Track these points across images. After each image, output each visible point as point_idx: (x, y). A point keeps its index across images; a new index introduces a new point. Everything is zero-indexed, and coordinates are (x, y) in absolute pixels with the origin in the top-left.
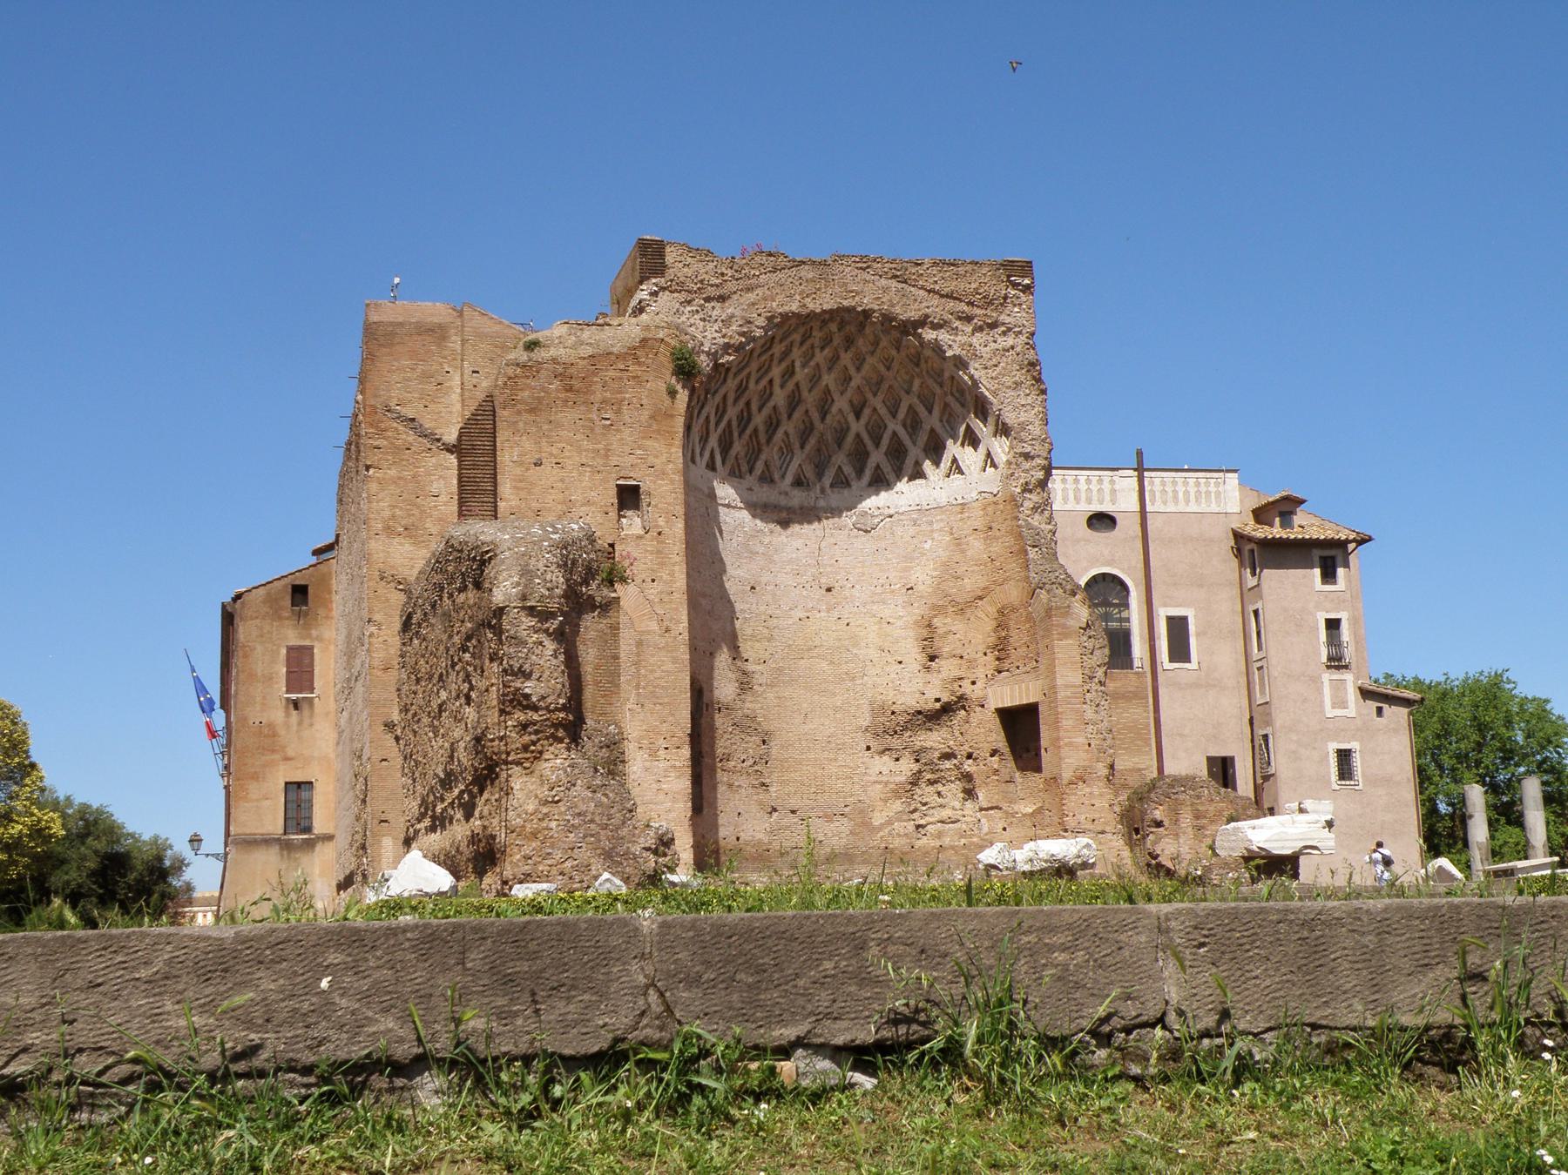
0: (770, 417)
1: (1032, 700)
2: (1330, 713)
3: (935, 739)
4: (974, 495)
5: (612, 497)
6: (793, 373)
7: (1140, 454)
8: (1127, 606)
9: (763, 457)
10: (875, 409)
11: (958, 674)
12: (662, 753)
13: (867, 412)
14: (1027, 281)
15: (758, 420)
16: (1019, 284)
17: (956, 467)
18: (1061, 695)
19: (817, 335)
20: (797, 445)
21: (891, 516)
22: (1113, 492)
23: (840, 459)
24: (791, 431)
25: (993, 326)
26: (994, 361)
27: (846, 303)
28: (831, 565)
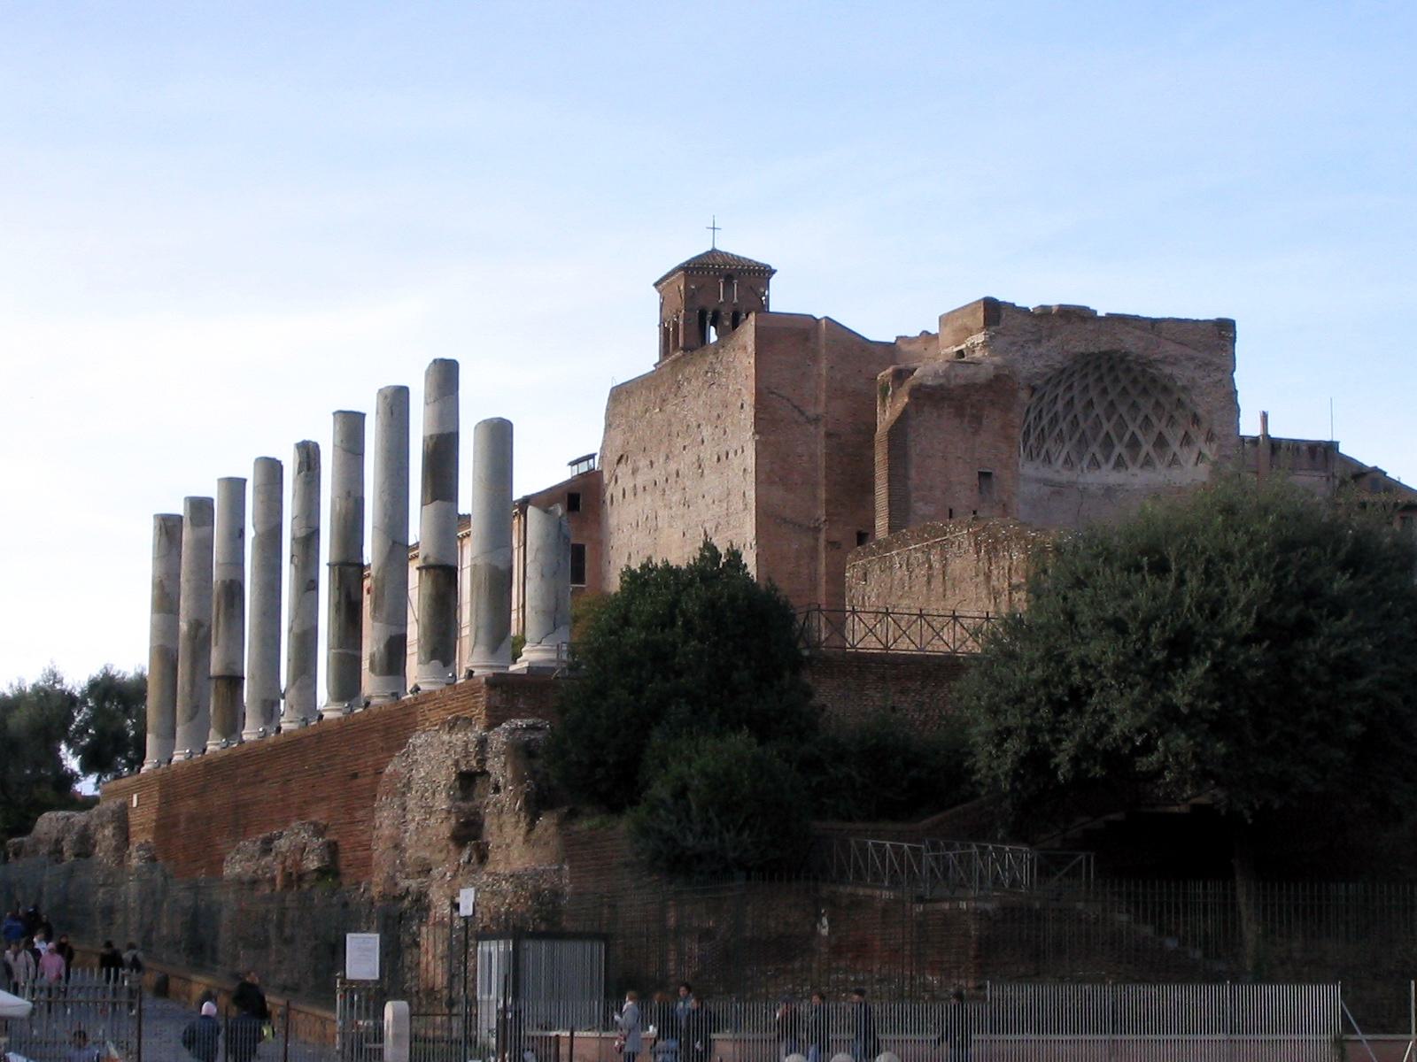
0: (1052, 418)
9: (1045, 447)
10: (1121, 416)
13: (1115, 417)
14: (1231, 335)
15: (1045, 421)
16: (1224, 336)
17: (1174, 461)
20: (1067, 438)
23: (1095, 448)
24: (1065, 428)
25: (1207, 364)
26: (1208, 390)
27: (1115, 347)
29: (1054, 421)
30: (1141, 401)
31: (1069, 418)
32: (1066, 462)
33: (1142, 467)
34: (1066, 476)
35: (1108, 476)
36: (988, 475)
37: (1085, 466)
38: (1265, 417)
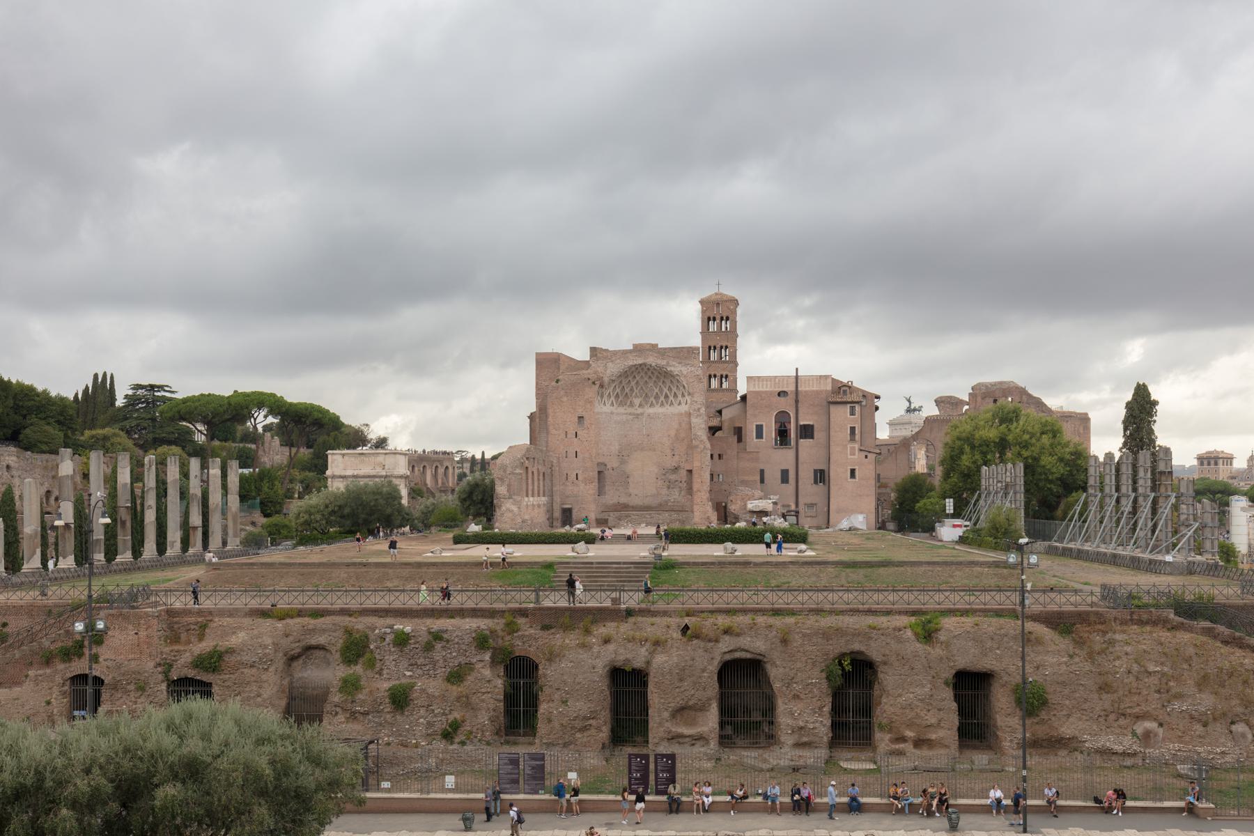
2: (849, 457)
3: (673, 477)
7: (797, 369)
19: (640, 369)
23: (652, 399)
29: (632, 390)
30: (666, 380)
32: (640, 405)
34: (640, 411)
35: (657, 410)
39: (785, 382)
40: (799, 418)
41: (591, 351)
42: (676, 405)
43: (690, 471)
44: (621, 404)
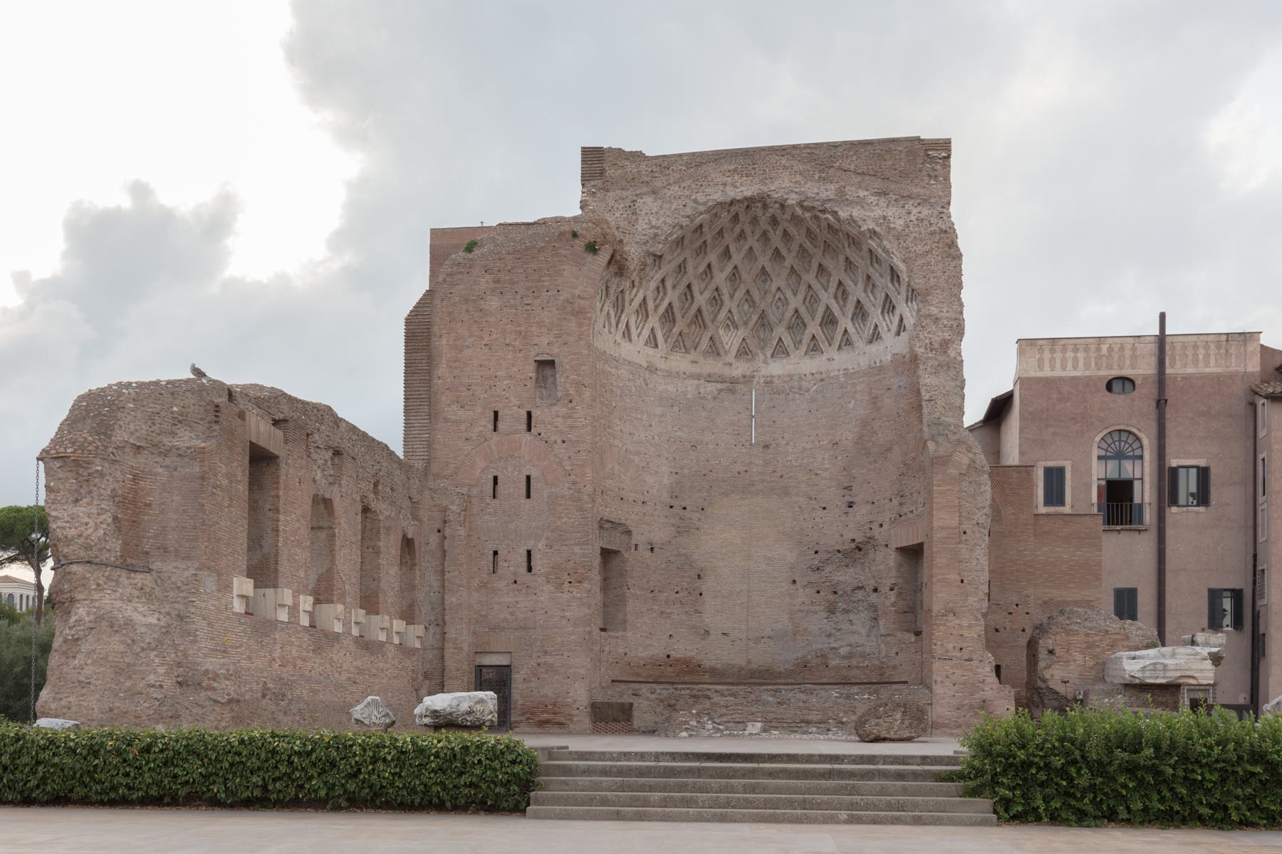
1: (920, 541)
4: (889, 358)
5: (530, 370)
6: (730, 257)
8: (1141, 457)
10: (810, 286)
11: (870, 518)
12: (567, 585)
18: (937, 535)
21: (822, 380)
22: (1134, 357)
23: (780, 331)
24: (735, 311)
28: (770, 426)
29: (716, 300)
31: (740, 294)
32: (744, 352)
33: (840, 348)
34: (740, 369)
35: (800, 364)
36: (551, 363)
37: (769, 355)
38: (1162, 317)
39: (1128, 353)
40: (1168, 450)
41: (584, 161)
42: (860, 344)
43: (914, 553)
44: (681, 344)
